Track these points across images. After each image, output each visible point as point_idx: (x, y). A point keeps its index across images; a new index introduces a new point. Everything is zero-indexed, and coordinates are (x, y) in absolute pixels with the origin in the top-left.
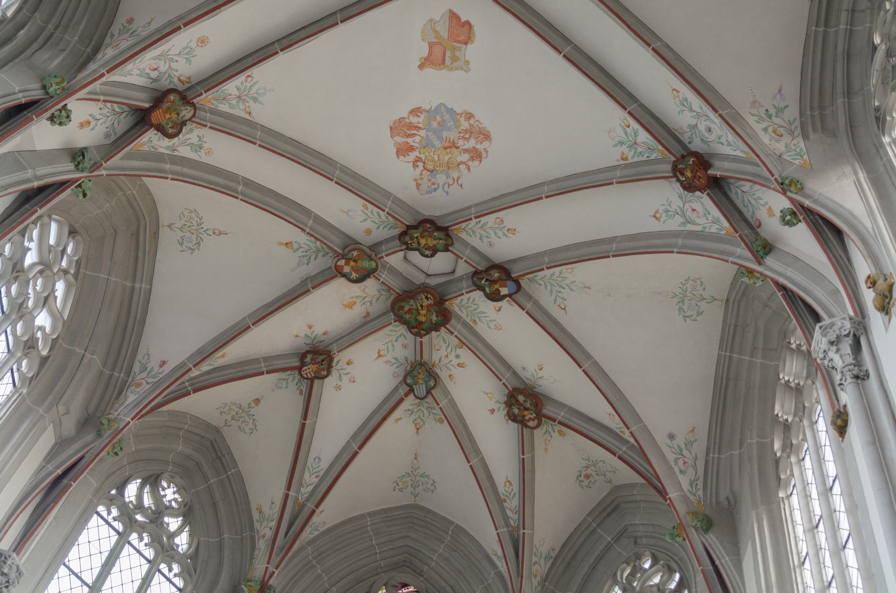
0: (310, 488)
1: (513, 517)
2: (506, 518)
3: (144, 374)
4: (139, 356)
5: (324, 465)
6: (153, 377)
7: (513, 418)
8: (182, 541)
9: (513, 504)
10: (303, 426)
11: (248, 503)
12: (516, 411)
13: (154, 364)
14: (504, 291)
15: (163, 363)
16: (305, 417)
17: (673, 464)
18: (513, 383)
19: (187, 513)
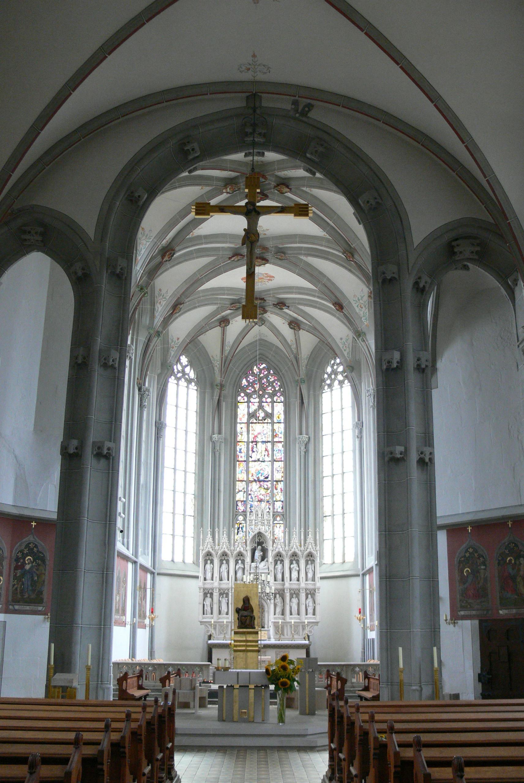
0: (228, 351)
1: (295, 351)
2: (292, 351)
3: (173, 343)
4: (170, 337)
5: (231, 343)
6: (177, 344)
7: (291, 328)
8: (192, 375)
9: (293, 347)
10: (223, 338)
11: (208, 355)
12: (292, 326)
13: (175, 339)
14: (284, 308)
15: (178, 339)
16: (223, 336)
17: (342, 348)
18: (290, 319)
19: (191, 363)
